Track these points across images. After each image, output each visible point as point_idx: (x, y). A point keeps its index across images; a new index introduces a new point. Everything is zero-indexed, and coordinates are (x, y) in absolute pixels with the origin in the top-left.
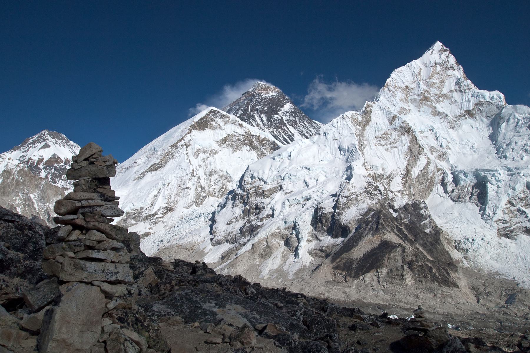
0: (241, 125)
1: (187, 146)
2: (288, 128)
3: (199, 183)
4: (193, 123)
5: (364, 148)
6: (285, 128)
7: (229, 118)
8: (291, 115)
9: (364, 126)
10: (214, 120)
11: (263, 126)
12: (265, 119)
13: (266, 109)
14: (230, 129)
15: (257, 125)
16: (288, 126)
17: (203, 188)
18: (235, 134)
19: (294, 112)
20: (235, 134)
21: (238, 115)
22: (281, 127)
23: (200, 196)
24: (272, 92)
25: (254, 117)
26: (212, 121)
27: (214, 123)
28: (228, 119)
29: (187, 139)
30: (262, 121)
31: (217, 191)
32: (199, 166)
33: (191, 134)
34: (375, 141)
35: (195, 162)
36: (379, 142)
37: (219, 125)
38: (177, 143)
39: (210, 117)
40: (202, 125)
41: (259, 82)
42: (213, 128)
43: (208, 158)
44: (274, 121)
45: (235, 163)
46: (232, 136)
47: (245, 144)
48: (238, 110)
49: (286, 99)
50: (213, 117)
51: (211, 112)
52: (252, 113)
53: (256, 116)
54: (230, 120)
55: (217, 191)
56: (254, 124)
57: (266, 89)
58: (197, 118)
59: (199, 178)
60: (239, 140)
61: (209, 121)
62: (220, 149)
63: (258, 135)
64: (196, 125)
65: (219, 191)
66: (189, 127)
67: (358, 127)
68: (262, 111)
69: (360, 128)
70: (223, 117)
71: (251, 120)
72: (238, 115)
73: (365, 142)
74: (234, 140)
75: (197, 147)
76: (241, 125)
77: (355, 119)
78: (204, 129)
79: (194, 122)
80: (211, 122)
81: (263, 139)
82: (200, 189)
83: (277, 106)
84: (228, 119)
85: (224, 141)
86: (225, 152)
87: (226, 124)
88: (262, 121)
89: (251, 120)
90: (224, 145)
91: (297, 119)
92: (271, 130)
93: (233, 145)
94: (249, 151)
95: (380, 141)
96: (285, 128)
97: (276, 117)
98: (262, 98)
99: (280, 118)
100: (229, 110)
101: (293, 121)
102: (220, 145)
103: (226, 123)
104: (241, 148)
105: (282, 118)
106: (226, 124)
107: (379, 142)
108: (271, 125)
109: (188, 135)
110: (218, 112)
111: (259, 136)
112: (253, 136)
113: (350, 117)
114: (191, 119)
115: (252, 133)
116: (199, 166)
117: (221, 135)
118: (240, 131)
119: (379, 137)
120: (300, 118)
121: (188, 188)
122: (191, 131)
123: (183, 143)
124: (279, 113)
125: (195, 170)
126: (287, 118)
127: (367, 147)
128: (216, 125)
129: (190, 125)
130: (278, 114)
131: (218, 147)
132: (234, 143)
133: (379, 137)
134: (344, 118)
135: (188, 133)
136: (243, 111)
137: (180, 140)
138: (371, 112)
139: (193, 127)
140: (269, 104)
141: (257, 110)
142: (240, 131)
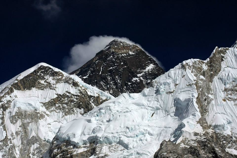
0: (75, 84)
4: (16, 81)
5: (209, 103)
7: (62, 75)
9: (212, 76)
18: (68, 94)
20: (68, 94)
21: (84, 77)
26: (42, 79)
27: (42, 82)
28: (60, 77)
30: (116, 84)
33: (12, 95)
34: (222, 95)
35: (13, 128)
36: (230, 96)
39: (39, 74)
40: (27, 84)
42: (42, 88)
44: (131, 85)
46: (64, 96)
47: (79, 107)
50: (42, 74)
51: (40, 68)
54: (64, 78)
60: (72, 101)
61: (37, 79)
62: (48, 113)
63: (96, 95)
64: (20, 85)
67: (202, 77)
69: (204, 79)
70: (54, 74)
72: (84, 77)
73: (210, 96)
74: (66, 101)
76: (75, 84)
77: (199, 68)
78: (29, 88)
79: (17, 80)
83: (138, 68)
84: (60, 77)
87: (57, 83)
89: (102, 83)
90: (53, 108)
93: (64, 108)
95: (231, 95)
97: (135, 79)
98: (118, 57)
102: (47, 108)
103: (58, 81)
104: (73, 111)
106: (57, 83)
107: (230, 96)
111: (98, 97)
113: (191, 64)
114: (14, 79)
115: (89, 93)
117: (51, 95)
118: (73, 91)
119: (230, 90)
127: (213, 102)
128: (45, 84)
130: (137, 77)
131: (45, 110)
132: (65, 105)
133: (230, 90)
135: (8, 93)
136: (92, 72)
138: (222, 60)
139: (17, 86)
141: (111, 71)
142: (73, 91)
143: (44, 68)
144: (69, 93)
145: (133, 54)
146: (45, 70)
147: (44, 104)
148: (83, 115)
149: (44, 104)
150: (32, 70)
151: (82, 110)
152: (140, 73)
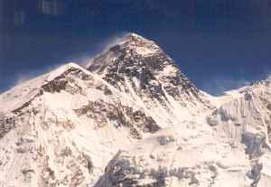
0: (108, 92)
1: (36, 113)
2: (166, 99)
3: (48, 164)
6: (162, 98)
8: (171, 82)
10: (73, 81)
11: (134, 93)
12: (137, 83)
13: (140, 70)
14: (94, 95)
15: (127, 91)
16: (166, 94)
17: (52, 173)
19: (176, 78)
22: (157, 96)
23: (47, 183)
24: (146, 49)
25: (123, 79)
27: (73, 85)
28: (90, 81)
29: (35, 104)
30: (133, 85)
31: (69, 178)
32: (49, 141)
33: (42, 97)
37: (80, 88)
38: (20, 108)
40: (56, 86)
41: (134, 35)
43: (61, 131)
45: (103, 144)
47: (112, 117)
48: (102, 69)
49: (168, 60)
51: (70, 70)
52: (121, 75)
53: (126, 78)
55: (69, 178)
56: (122, 87)
57: (142, 44)
58: (52, 75)
59: (48, 157)
65: (72, 179)
66: (39, 87)
68: (135, 74)
70: (85, 77)
71: (119, 83)
75: (49, 115)
76: (108, 92)
78: (58, 91)
80: (70, 83)
81: (137, 113)
82: (47, 173)
84: (90, 81)
85: (84, 111)
86: (85, 125)
88: (133, 85)
90: (85, 116)
91: (180, 88)
92: (145, 98)
93: (95, 117)
94: (117, 127)
96: (162, 98)
97: (152, 82)
99: (157, 84)
100: (91, 67)
101: (174, 90)
102: (79, 116)
105: (160, 85)
108: (145, 93)
109: (38, 98)
110: (80, 71)
112: (123, 107)
116: (49, 141)
117: (83, 102)
120: (184, 86)
121: (32, 171)
122: (41, 93)
123: (30, 107)
124: (157, 77)
125: (43, 146)
126: (167, 84)
129: (41, 85)
130: (154, 79)
132: (96, 114)
134: (248, 97)
135: (38, 95)
137: (27, 105)
140: (144, 65)
141: (128, 70)
143: (74, 70)
144: (102, 101)
145: (152, 52)
146: (77, 72)
147: (76, 111)
148: (117, 127)
149: (76, 111)
150: (62, 69)
151: (115, 122)
152: (157, 74)
